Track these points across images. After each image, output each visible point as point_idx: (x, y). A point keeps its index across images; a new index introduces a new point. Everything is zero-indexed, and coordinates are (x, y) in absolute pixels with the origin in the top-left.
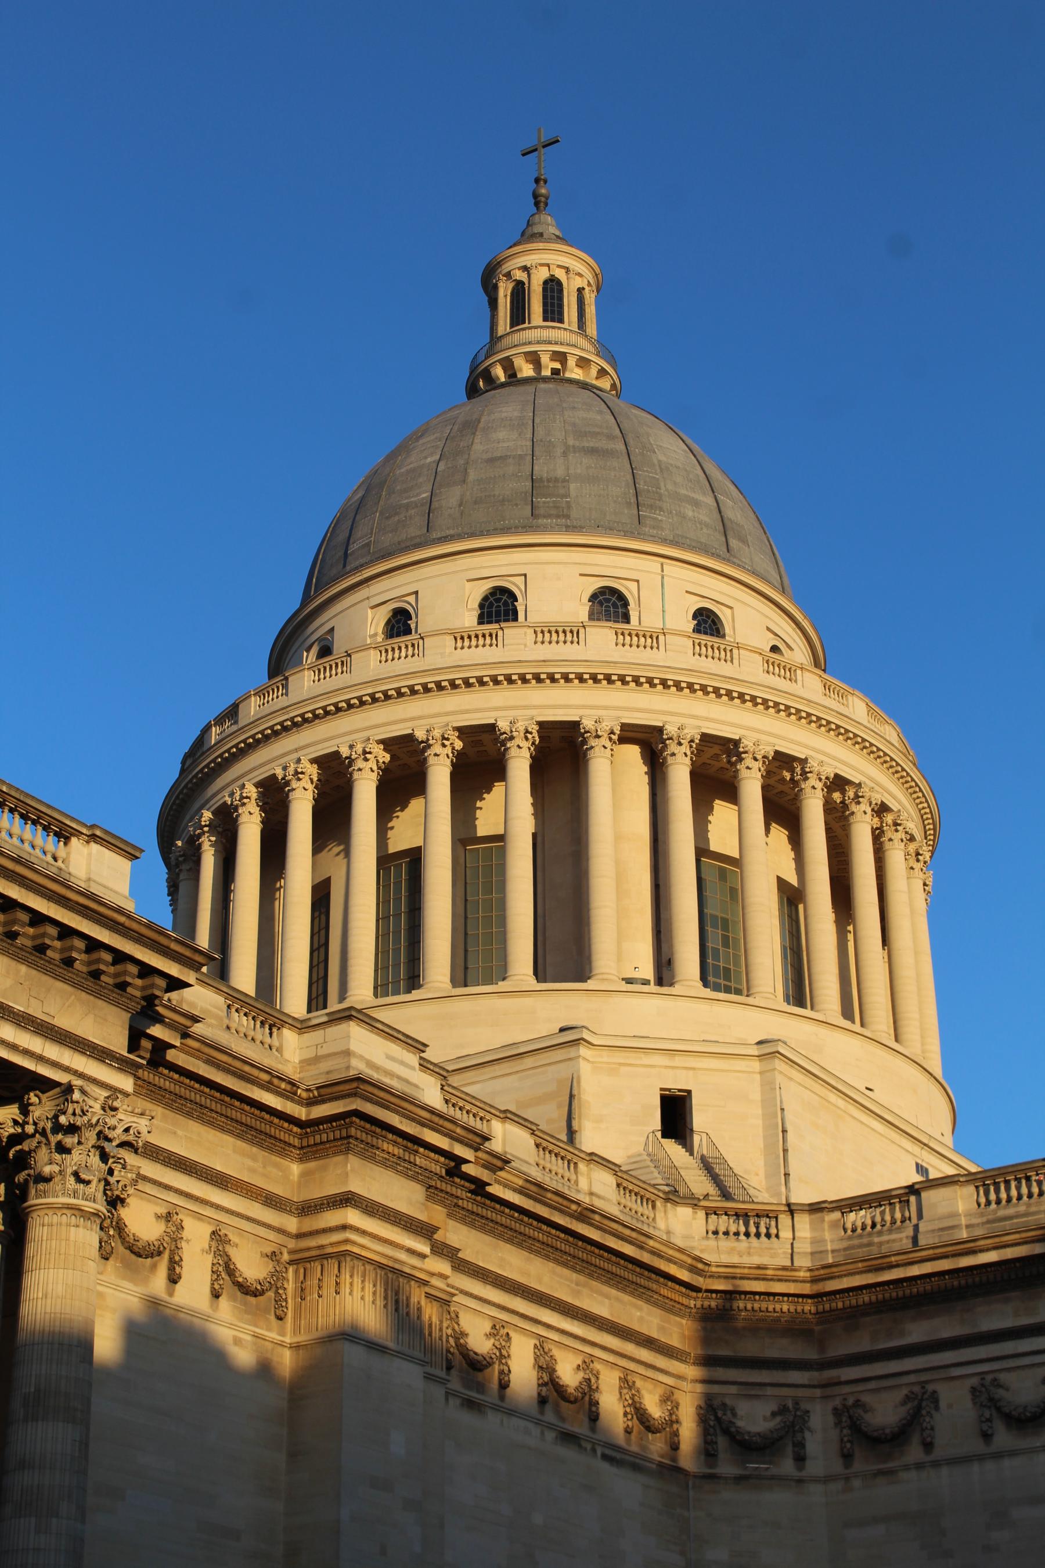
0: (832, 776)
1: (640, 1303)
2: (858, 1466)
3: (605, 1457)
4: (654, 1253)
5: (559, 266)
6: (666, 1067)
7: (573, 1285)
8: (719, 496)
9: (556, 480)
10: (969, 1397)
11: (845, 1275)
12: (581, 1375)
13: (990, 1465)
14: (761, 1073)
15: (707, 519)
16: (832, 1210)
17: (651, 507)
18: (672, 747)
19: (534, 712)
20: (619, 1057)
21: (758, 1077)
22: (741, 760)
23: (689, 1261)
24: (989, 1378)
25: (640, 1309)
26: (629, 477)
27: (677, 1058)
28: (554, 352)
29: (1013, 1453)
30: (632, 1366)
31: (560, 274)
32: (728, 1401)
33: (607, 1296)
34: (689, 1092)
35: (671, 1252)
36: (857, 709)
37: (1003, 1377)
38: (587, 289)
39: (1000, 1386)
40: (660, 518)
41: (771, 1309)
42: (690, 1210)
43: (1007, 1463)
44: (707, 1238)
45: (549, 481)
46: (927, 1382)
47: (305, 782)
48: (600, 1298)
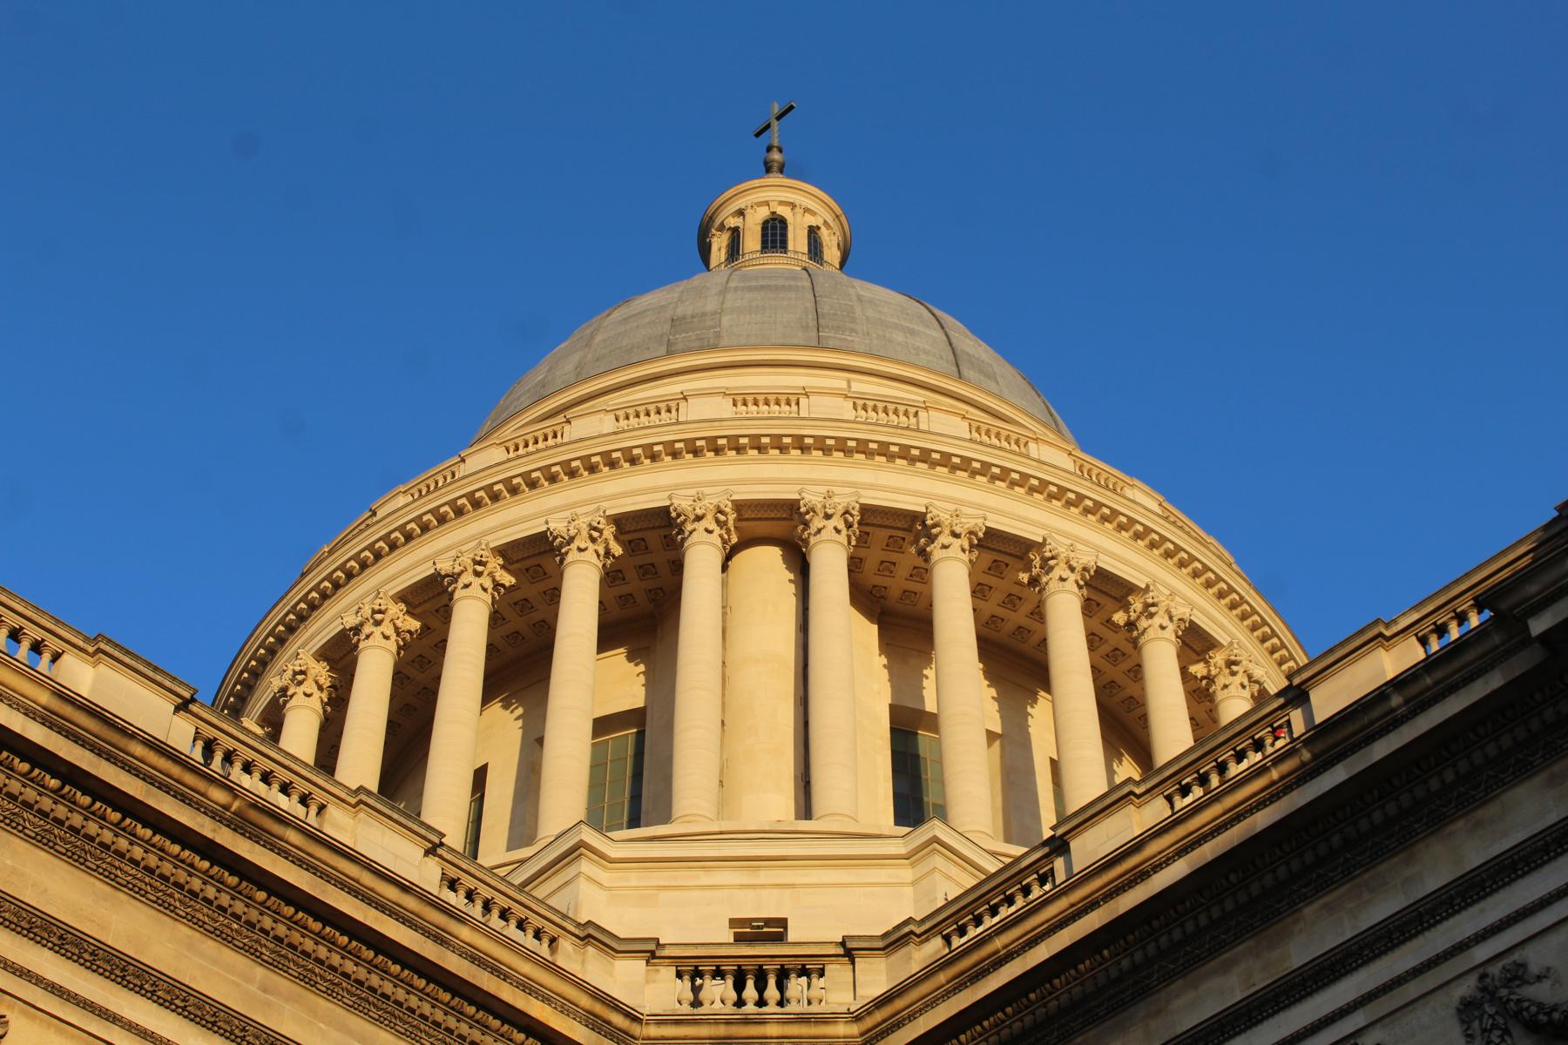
4: (477, 958)
5: (781, 203)
6: (742, 886)
7: (253, 988)
8: (951, 333)
9: (704, 314)
11: (921, 1011)
14: (914, 883)
15: (928, 347)
16: (924, 937)
18: (817, 523)
20: (662, 877)
21: (909, 891)
22: (932, 539)
26: (810, 305)
27: (762, 873)
31: (783, 211)
36: (1142, 501)
38: (824, 233)
42: (639, 965)
47: (309, 686)
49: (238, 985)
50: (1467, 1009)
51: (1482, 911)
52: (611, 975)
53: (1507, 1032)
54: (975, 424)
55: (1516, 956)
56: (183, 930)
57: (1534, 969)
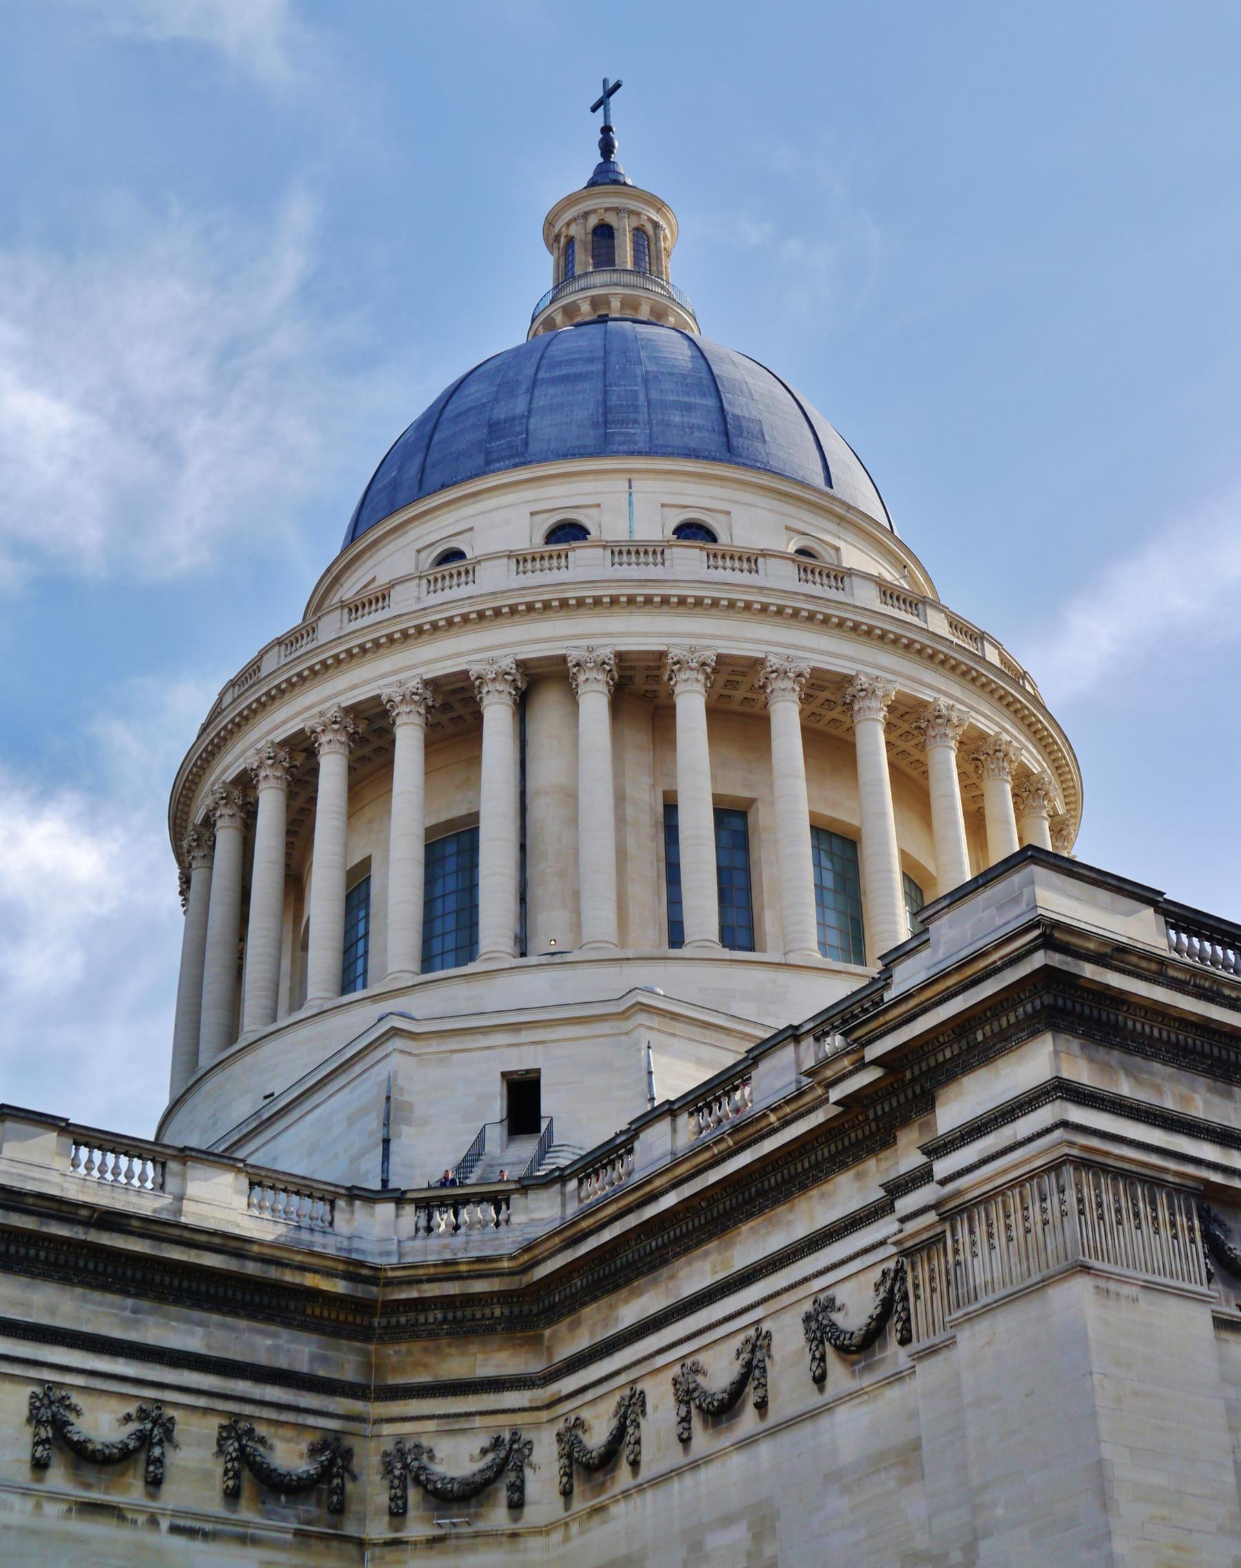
0: (807, 672)
1: (273, 1328)
2: (580, 1504)
3: (174, 1529)
7: (127, 1314)
9: (514, 418)
10: (671, 1389)
12: (134, 1426)
13: (688, 1480)
15: (701, 422)
17: (622, 422)
19: (421, 670)
20: (453, 1044)
23: (341, 1267)
24: (689, 1362)
25: (274, 1335)
28: (593, 297)
29: (708, 1460)
30: (247, 1409)
32: (425, 1442)
33: (200, 1324)
34: (538, 1071)
35: (299, 1258)
37: (702, 1358)
39: (697, 1371)
40: (632, 431)
41: (478, 1315)
43: (704, 1474)
44: (414, 1238)
45: (505, 421)
46: (634, 1381)
48: (183, 1326)
49: (116, 1315)
50: (808, 1319)
51: (817, 1259)
52: (373, 1215)
53: (822, 1342)
54: (712, 553)
55: (829, 1293)
56: (79, 1291)
57: (838, 1303)
